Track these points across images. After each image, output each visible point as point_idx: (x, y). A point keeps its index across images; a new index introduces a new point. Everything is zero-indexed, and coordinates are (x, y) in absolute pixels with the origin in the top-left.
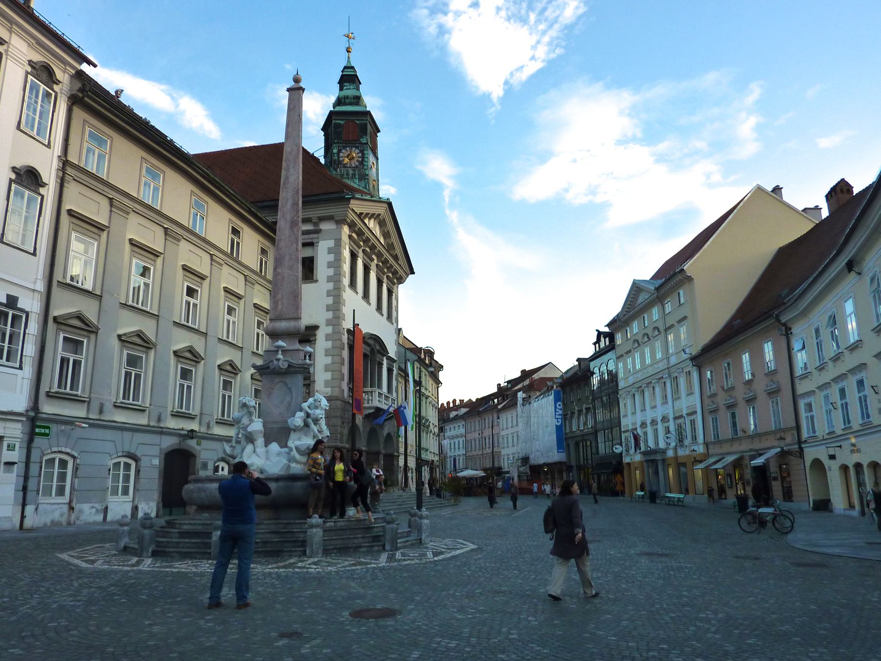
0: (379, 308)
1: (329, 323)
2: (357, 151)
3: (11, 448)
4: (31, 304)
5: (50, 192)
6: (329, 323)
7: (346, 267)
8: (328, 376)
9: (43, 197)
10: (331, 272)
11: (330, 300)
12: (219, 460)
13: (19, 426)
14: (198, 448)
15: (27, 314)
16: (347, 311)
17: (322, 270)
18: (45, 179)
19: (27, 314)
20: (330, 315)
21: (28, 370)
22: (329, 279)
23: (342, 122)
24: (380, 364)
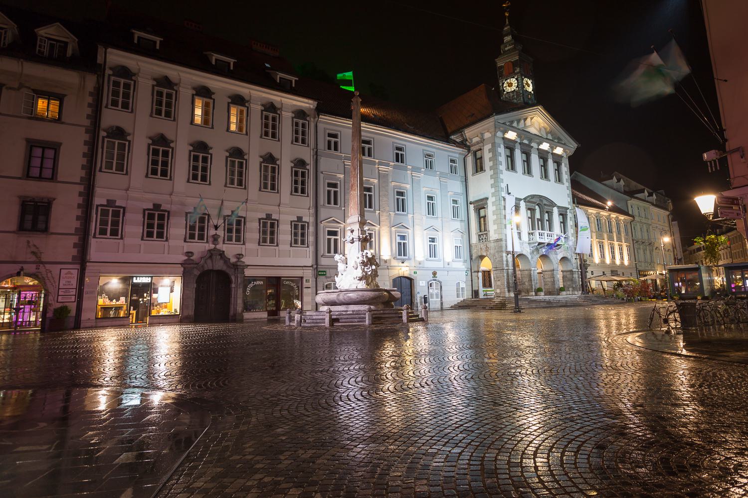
0: (545, 176)
1: (493, 195)
2: (514, 79)
3: (307, 281)
4: (308, 218)
5: (311, 167)
6: (493, 195)
7: (502, 159)
8: (495, 227)
9: (308, 170)
10: (491, 164)
11: (492, 181)
12: (431, 280)
13: (310, 271)
14: (415, 275)
15: (308, 223)
16: (503, 185)
17: (487, 164)
18: (308, 161)
19: (308, 223)
20: (493, 190)
21: (312, 248)
22: (491, 168)
23: (503, 64)
24: (550, 213)
